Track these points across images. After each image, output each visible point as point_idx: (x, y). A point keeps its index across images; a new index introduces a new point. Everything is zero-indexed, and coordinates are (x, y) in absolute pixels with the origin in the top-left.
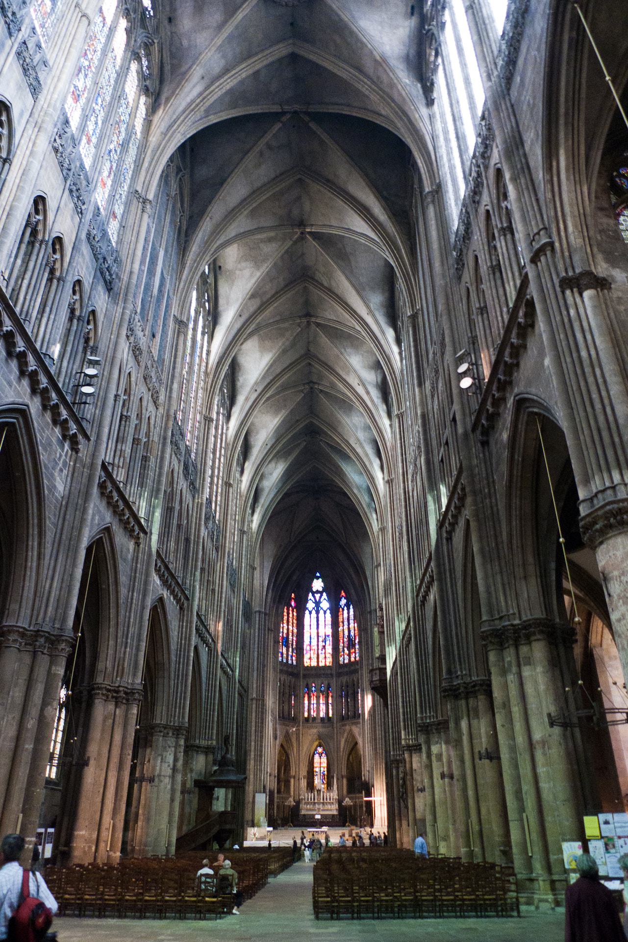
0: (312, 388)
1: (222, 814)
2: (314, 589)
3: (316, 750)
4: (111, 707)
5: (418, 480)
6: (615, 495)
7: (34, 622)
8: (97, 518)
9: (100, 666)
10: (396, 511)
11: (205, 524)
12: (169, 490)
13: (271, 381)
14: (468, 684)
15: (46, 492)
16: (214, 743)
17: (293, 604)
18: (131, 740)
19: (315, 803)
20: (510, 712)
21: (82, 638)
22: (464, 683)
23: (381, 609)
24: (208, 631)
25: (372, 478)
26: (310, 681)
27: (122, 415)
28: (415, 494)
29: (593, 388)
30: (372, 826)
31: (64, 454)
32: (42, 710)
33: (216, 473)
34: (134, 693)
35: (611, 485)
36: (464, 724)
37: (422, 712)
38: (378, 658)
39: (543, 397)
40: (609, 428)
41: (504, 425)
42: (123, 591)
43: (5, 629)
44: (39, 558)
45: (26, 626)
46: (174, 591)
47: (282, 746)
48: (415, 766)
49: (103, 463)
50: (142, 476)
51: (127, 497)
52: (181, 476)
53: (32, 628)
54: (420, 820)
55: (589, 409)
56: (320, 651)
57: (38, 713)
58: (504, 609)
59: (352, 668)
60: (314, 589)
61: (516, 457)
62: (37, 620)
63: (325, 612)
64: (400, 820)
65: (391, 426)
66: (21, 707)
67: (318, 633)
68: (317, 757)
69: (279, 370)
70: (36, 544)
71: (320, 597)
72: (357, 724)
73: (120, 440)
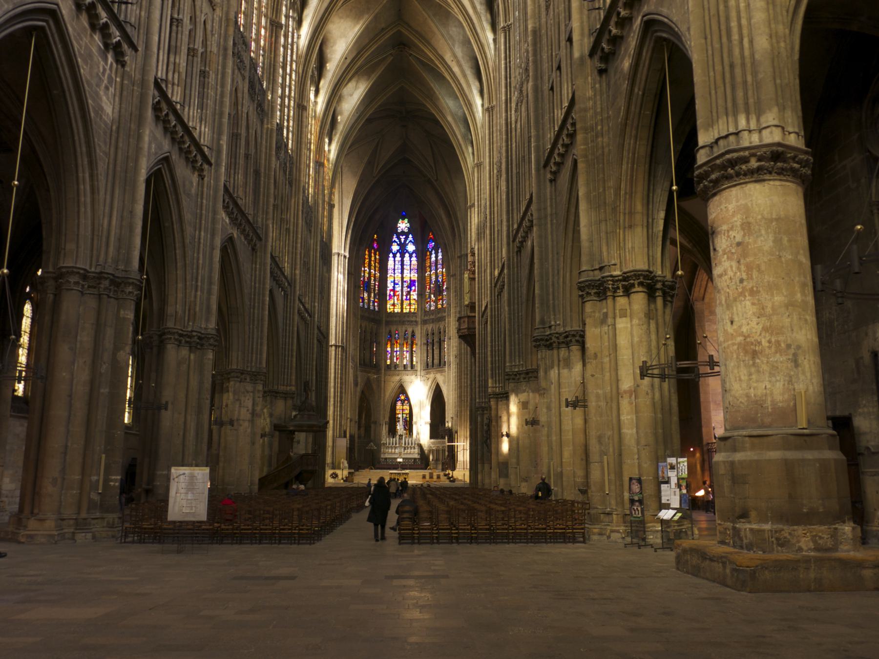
2: (399, 230)
3: (399, 397)
4: (184, 352)
5: (523, 109)
6: (738, 142)
8: (153, 146)
9: (170, 310)
10: (495, 145)
11: (277, 154)
12: (233, 113)
14: (560, 334)
15: (92, 114)
16: (293, 388)
18: (208, 385)
19: (395, 448)
21: (148, 280)
22: (557, 333)
23: (473, 254)
24: (283, 274)
25: (470, 105)
26: (393, 328)
27: (172, 19)
28: (519, 126)
29: (733, 14)
30: (454, 468)
31: (108, 68)
32: (114, 355)
33: (287, 93)
34: (209, 338)
35: (735, 131)
37: (511, 361)
38: (467, 306)
39: (675, 19)
40: (743, 65)
41: (626, 50)
42: (189, 230)
43: (64, 270)
44: (93, 192)
45: (88, 268)
46: (244, 230)
47: (363, 392)
49: (156, 79)
50: (202, 96)
51: (186, 121)
52: (246, 95)
53: (93, 270)
54: (503, 463)
55: (724, 40)
56: (404, 297)
58: (606, 260)
59: (438, 316)
60: (399, 230)
61: (636, 90)
62: (98, 261)
64: (483, 463)
65: (495, 40)
67: (402, 278)
70: (87, 175)
71: (406, 239)
72: (442, 372)
73: (172, 49)
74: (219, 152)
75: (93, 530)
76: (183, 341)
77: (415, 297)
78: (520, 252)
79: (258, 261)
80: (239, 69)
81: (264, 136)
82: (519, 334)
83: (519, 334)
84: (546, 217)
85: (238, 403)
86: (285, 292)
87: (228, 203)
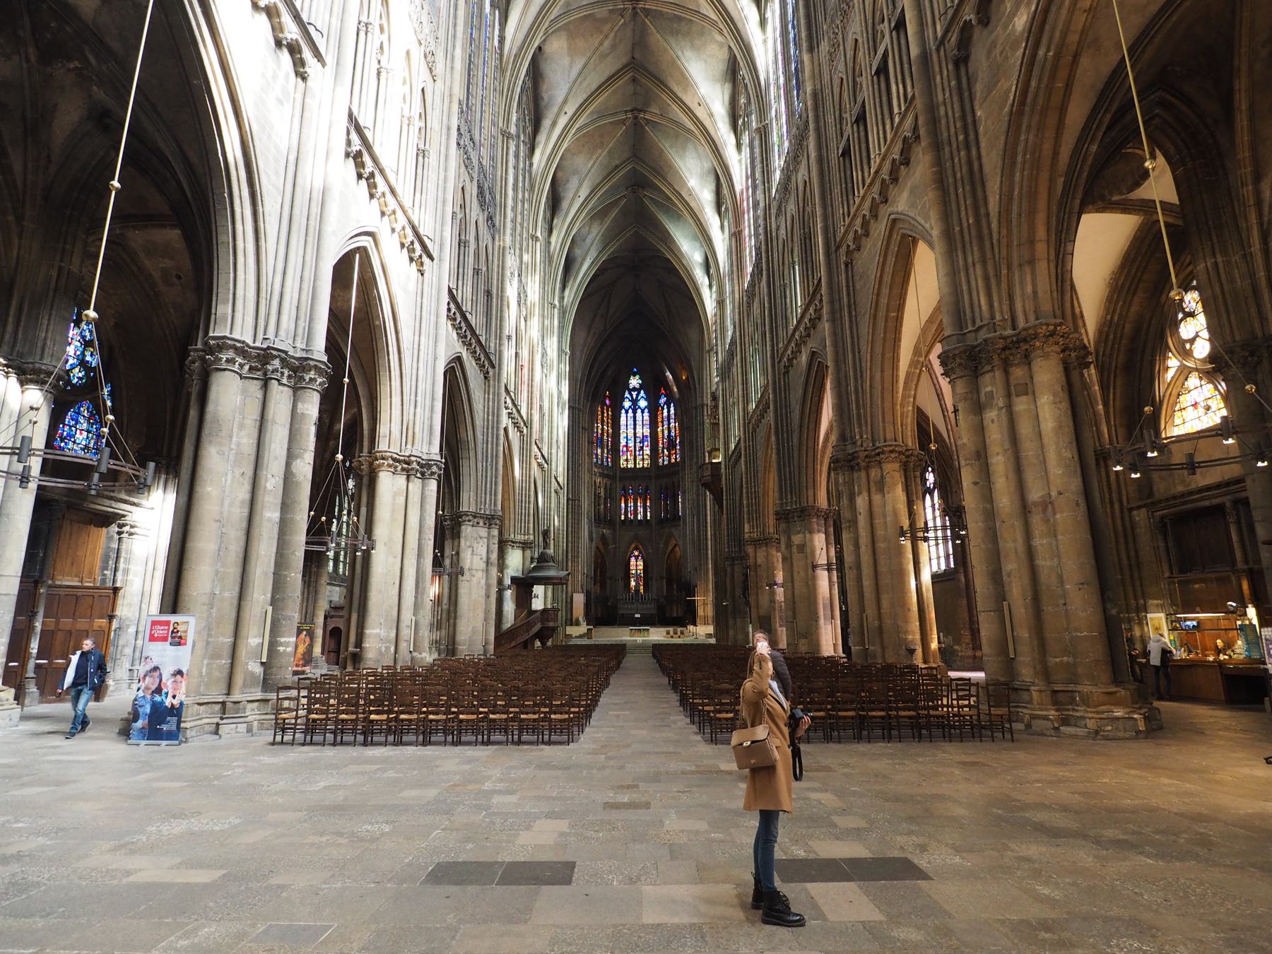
0: (636, 118)
1: (545, 611)
2: (631, 386)
4: (401, 480)
7: (260, 336)
12: (460, 216)
13: (585, 101)
16: (532, 537)
17: (607, 402)
20: (987, 465)
23: (715, 398)
32: (288, 465)
34: (431, 465)
36: (861, 502)
47: (598, 548)
48: (759, 561)
53: (258, 344)
57: (283, 469)
60: (631, 386)
63: (643, 412)
64: (735, 618)
66: (253, 458)
67: (635, 434)
68: (633, 560)
69: (594, 86)
71: (637, 395)
74: (441, 245)
75: (250, 719)
76: (399, 468)
77: (648, 452)
78: (787, 372)
79: (491, 390)
80: (466, 167)
81: (496, 253)
82: (790, 467)
83: (790, 467)
84: (841, 309)
85: (470, 550)
86: (521, 432)
87: (454, 314)
